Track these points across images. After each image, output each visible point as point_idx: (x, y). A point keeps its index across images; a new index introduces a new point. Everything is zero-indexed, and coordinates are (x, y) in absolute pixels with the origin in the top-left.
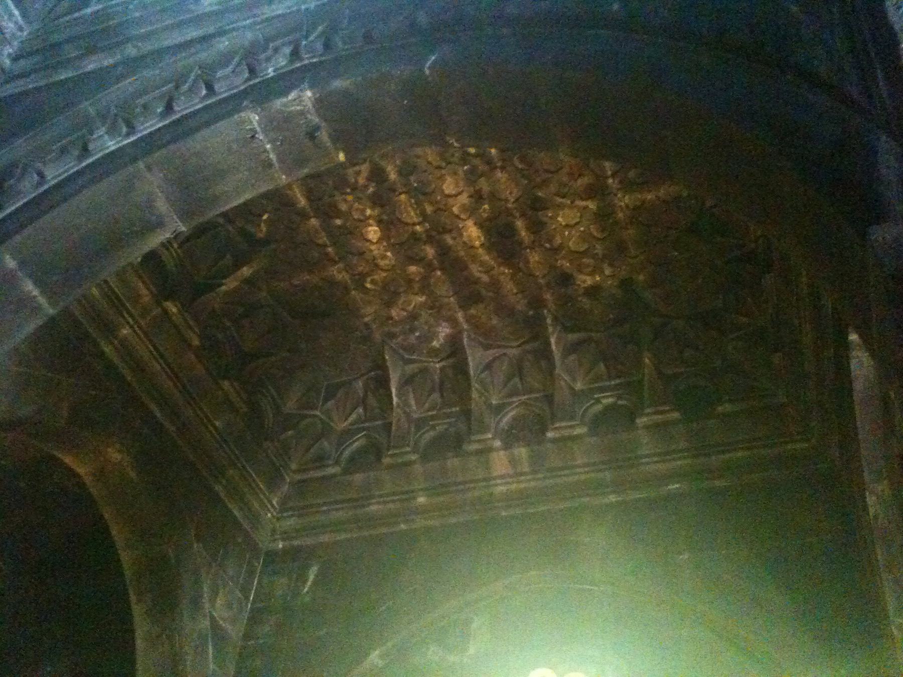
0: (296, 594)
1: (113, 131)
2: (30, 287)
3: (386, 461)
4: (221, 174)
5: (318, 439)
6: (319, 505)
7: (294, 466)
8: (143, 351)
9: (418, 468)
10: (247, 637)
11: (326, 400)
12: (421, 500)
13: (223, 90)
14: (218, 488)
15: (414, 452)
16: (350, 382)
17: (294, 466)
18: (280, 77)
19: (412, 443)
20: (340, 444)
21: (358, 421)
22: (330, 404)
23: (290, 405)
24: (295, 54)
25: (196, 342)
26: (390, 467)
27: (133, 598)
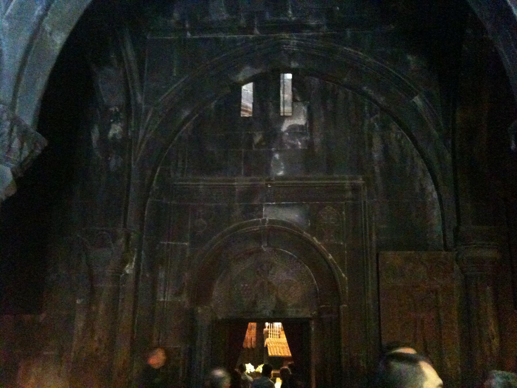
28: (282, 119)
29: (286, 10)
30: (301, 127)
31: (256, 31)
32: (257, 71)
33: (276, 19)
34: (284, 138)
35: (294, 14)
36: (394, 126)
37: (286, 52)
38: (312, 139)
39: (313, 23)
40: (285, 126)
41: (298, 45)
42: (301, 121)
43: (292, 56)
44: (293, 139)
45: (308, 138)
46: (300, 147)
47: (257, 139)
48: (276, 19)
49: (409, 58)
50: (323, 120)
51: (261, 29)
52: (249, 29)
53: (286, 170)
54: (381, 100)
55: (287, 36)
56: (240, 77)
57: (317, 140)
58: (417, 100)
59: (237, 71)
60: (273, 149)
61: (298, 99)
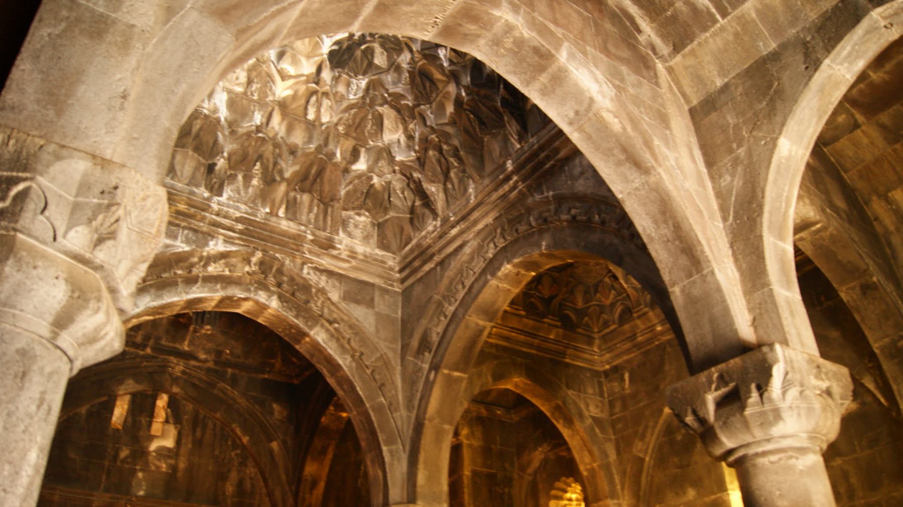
0: (623, 389)
1: (450, 304)
2: (456, 374)
3: (635, 315)
4: (494, 303)
5: (601, 313)
6: (615, 345)
7: (596, 330)
8: (505, 332)
9: (651, 314)
10: (612, 414)
11: (595, 294)
12: (659, 328)
13: (478, 270)
14: (567, 360)
15: (646, 306)
16: (601, 281)
17: (596, 330)
18: (495, 256)
19: (643, 302)
20: (611, 311)
21: (615, 297)
22: (598, 295)
23: (580, 304)
24: (496, 246)
25: (523, 313)
26: (639, 317)
27: (555, 423)
28: (151, 438)
29: (184, 340)
30: (169, 450)
31: (149, 351)
32: (139, 388)
33: (171, 344)
34: (150, 458)
35: (189, 346)
36: (250, 463)
37: (171, 375)
38: (177, 463)
39: (203, 356)
40: (154, 446)
41: (183, 372)
42: (169, 443)
43: (175, 380)
44: (159, 460)
45: (172, 462)
46: (164, 470)
47: (124, 453)
48: (171, 344)
49: (275, 406)
50: (190, 446)
51: (153, 349)
52: (143, 346)
53: (146, 491)
54: (245, 439)
55: (175, 361)
56: (121, 390)
57: (182, 465)
58: (275, 445)
59: (121, 382)
60: (138, 467)
61: (171, 420)
